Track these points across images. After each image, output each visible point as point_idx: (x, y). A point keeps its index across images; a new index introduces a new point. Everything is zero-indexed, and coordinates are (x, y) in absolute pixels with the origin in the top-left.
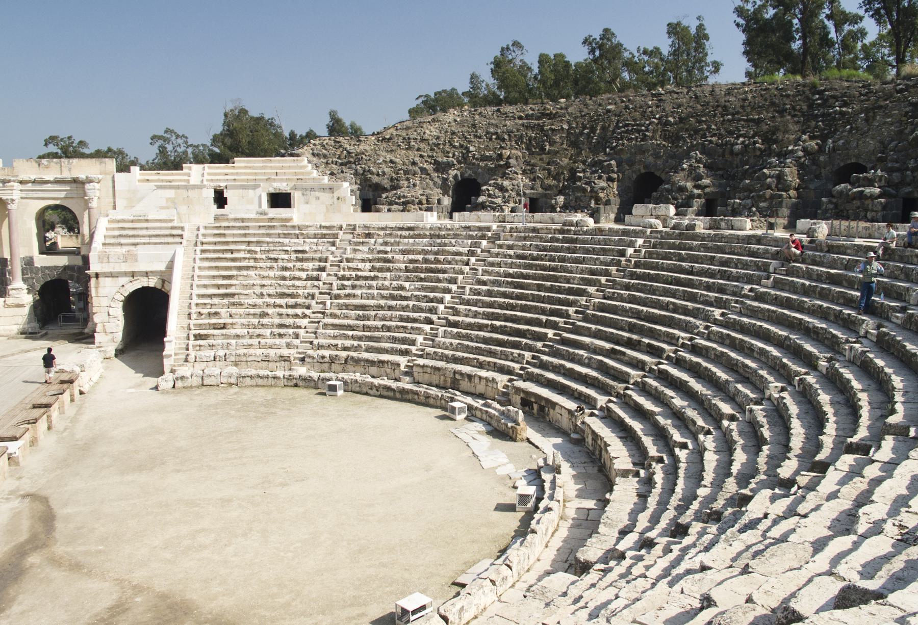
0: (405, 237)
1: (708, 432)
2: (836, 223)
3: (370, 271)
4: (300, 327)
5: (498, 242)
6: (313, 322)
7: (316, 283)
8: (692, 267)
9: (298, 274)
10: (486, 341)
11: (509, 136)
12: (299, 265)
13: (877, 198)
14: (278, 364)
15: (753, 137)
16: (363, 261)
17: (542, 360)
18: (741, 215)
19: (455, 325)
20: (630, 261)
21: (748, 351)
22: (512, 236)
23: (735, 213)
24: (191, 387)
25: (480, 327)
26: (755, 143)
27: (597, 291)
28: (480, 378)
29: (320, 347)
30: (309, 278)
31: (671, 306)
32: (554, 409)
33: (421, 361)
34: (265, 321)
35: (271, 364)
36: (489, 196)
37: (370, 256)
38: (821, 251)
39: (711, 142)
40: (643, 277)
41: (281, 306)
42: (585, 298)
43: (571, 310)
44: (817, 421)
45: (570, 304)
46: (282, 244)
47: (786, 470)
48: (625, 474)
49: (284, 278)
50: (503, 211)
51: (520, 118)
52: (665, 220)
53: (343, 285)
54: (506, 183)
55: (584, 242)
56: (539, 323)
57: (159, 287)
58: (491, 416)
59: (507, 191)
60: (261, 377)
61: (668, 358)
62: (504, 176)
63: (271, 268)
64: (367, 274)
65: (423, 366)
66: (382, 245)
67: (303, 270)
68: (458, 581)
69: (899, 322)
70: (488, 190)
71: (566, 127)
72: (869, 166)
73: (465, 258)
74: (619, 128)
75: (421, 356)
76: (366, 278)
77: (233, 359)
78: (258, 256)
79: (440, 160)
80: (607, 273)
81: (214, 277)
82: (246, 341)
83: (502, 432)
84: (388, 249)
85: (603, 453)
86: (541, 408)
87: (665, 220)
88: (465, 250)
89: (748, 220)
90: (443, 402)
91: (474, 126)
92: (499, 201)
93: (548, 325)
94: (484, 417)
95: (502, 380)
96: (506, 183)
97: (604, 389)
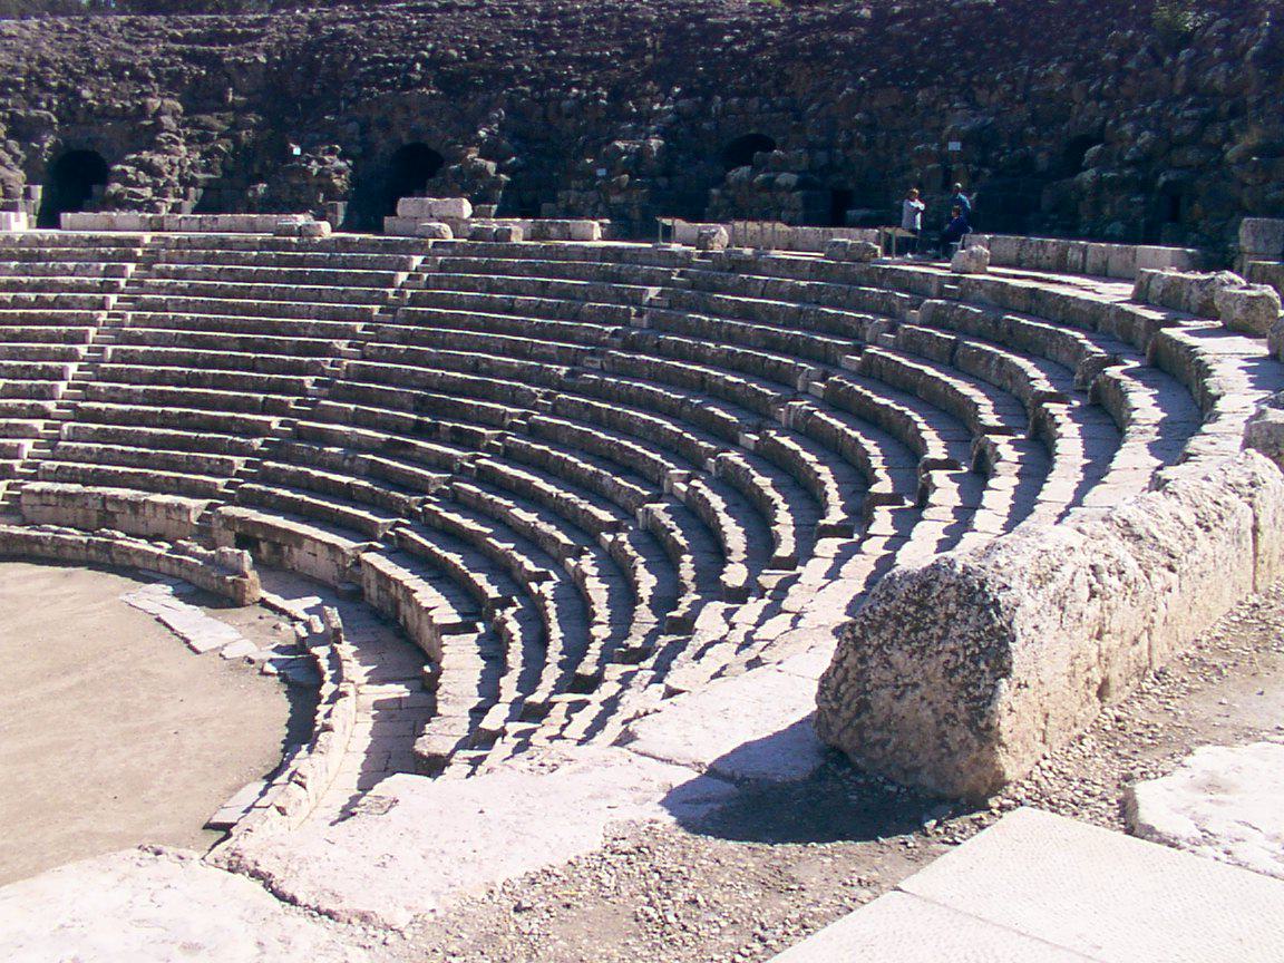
1: (545, 577)
2: (739, 225)
5: (157, 266)
8: (512, 300)
10: (155, 442)
11: (156, 72)
13: (794, 190)
15: (594, 87)
18: (580, 216)
19: (95, 416)
20: (403, 294)
21: (627, 429)
22: (182, 254)
23: (573, 212)
25: (143, 419)
26: (598, 97)
27: (350, 346)
28: (155, 505)
33: (37, 486)
36: (128, 183)
39: (523, 93)
40: (425, 318)
42: (330, 360)
43: (308, 381)
44: (757, 515)
45: (302, 370)
47: (735, 575)
48: (452, 629)
50: (157, 210)
51: (174, 39)
52: (455, 222)
54: (158, 159)
55: (315, 263)
56: (253, 407)
58: (191, 568)
59: (161, 174)
61: (490, 449)
62: (156, 147)
65: (41, 493)
68: (216, 819)
69: (854, 368)
70: (124, 172)
71: (262, 59)
72: (779, 140)
74: (364, 64)
75: (34, 478)
79: (21, 113)
80: (364, 316)
83: (214, 593)
85: (403, 607)
86: (277, 548)
87: (455, 222)
89: (596, 224)
90: (92, 552)
91: (85, 51)
92: (148, 193)
93: (267, 408)
94: (176, 569)
95: (196, 505)
96: (158, 159)
97: (387, 508)
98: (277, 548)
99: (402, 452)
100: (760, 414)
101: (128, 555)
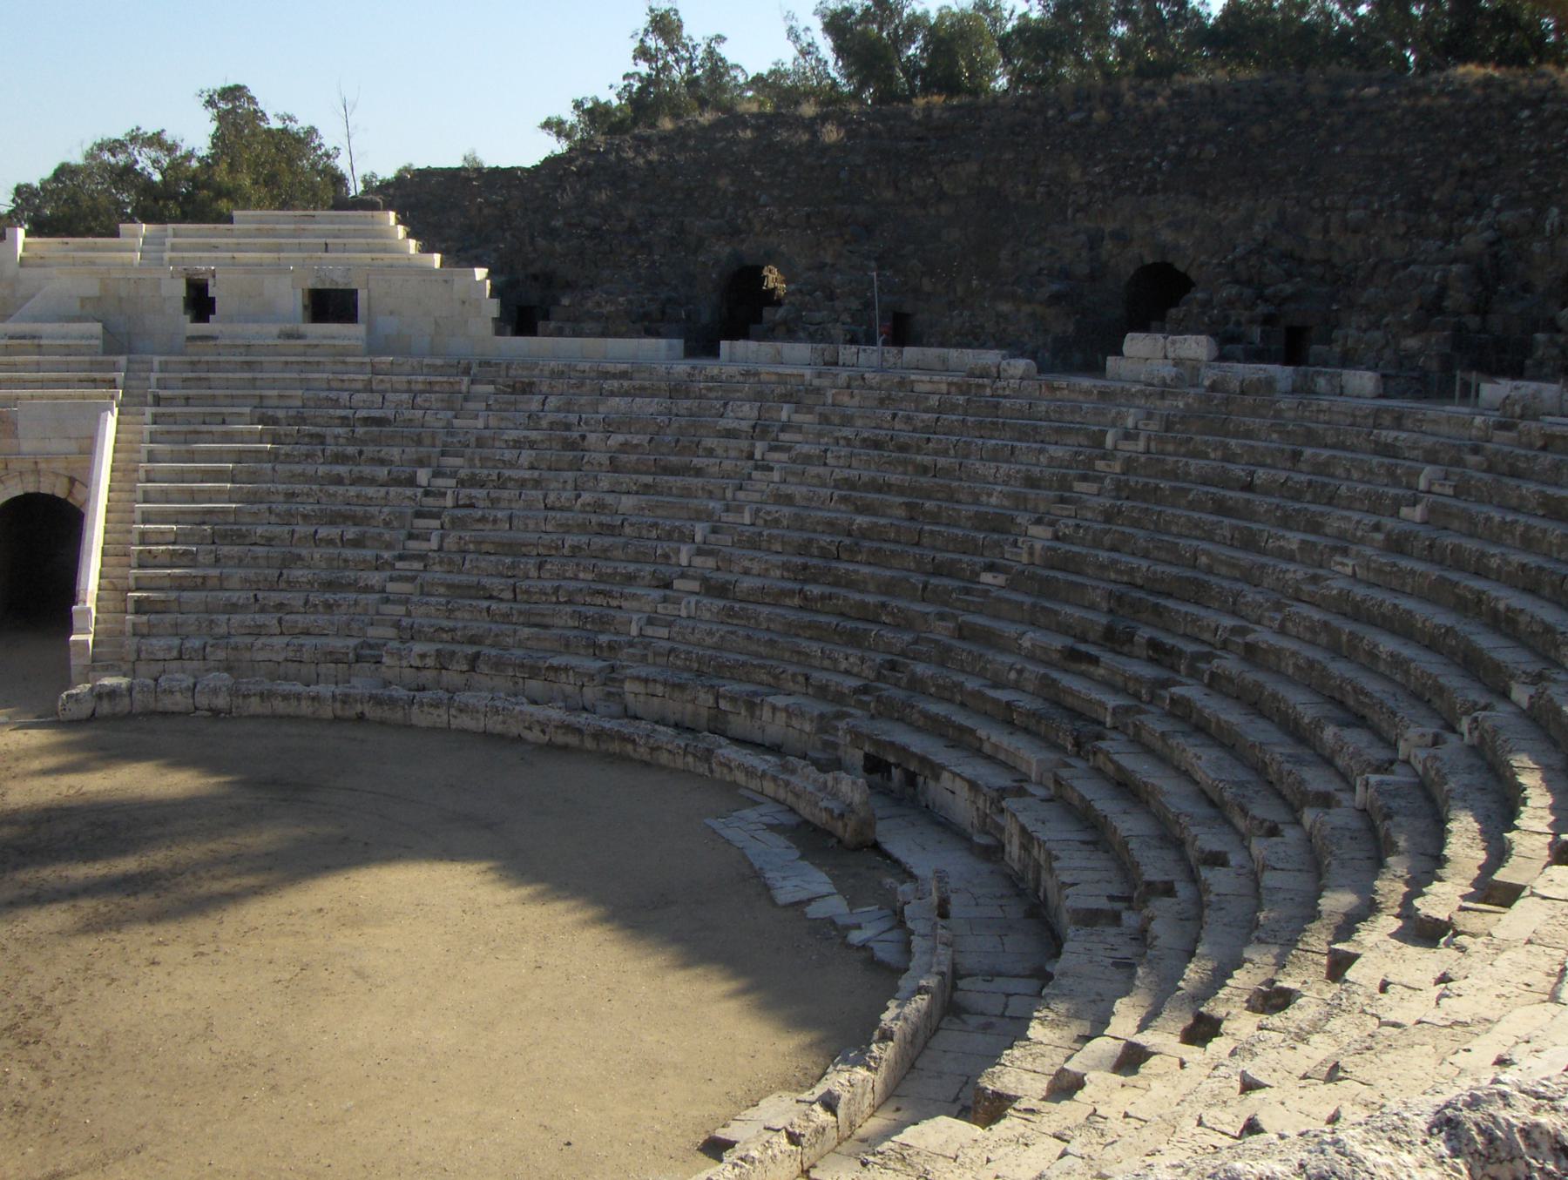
0: (612, 394)
3: (532, 468)
4: (368, 589)
6: (400, 579)
7: (409, 492)
9: (367, 470)
12: (369, 450)
14: (323, 668)
16: (518, 444)
17: (913, 674)
24: (130, 716)
28: (774, 708)
29: (413, 634)
30: (397, 482)
31: (1204, 560)
32: (937, 778)
34: (298, 573)
35: (304, 669)
37: (534, 435)
38: (1530, 446)
41: (330, 542)
46: (336, 403)
48: (1089, 918)
49: (339, 480)
53: (470, 498)
57: (61, 492)
60: (286, 697)
63: (308, 456)
64: (527, 474)
66: (558, 410)
67: (382, 462)
73: (744, 444)
76: (522, 483)
77: (221, 655)
78: (282, 429)
81: (181, 476)
82: (248, 618)
84: (573, 418)
85: (1044, 875)
86: (911, 778)
88: (745, 426)
98: (911, 778)
99: (1083, 667)
100: (1546, 658)
101: (731, 769)
